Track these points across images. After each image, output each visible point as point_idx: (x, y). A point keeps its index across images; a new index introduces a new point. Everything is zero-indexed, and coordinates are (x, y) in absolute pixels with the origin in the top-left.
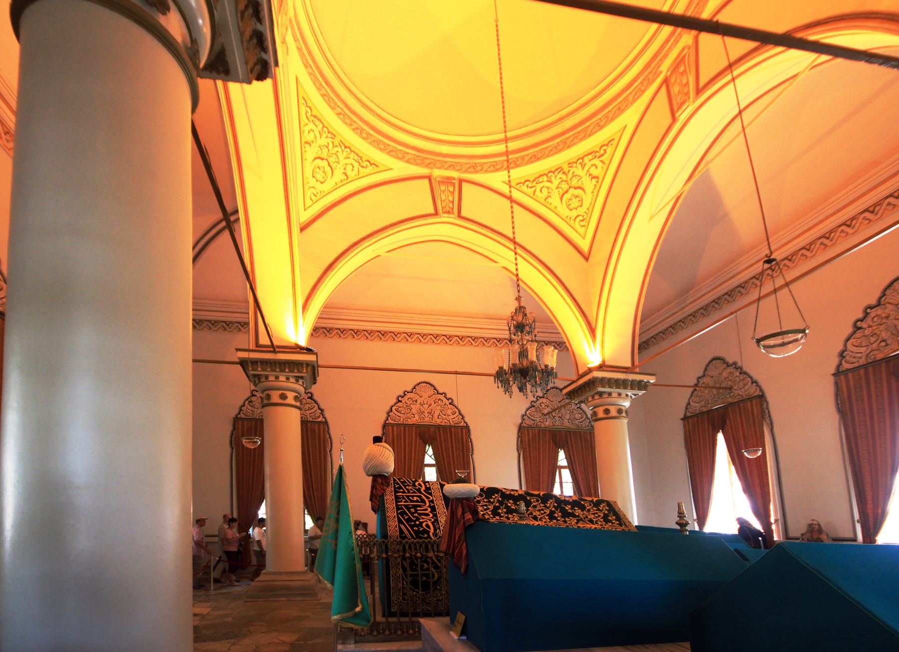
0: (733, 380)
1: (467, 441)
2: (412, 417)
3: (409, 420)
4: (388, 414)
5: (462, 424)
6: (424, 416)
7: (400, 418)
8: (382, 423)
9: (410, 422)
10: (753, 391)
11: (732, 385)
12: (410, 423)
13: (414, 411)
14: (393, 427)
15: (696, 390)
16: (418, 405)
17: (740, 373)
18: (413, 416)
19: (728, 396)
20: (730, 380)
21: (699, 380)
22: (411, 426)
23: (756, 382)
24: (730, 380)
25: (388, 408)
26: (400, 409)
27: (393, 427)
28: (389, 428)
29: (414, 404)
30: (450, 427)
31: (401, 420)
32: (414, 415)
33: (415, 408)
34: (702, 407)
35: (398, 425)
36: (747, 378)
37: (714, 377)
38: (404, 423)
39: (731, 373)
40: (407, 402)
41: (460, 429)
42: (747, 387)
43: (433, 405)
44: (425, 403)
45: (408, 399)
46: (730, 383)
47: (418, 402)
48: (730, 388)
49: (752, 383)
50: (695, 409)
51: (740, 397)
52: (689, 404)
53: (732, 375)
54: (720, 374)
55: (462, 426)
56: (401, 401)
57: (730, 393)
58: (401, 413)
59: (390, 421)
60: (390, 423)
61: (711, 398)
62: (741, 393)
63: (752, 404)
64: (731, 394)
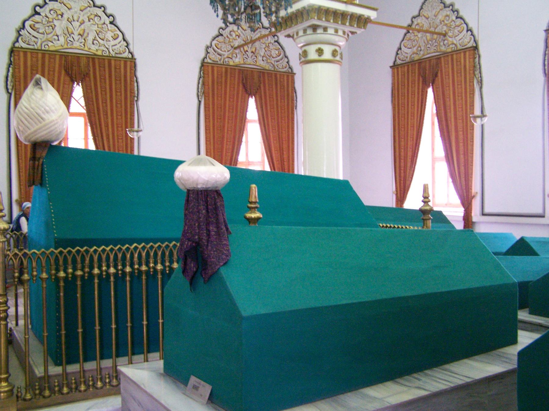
0: (449, 25)
1: (131, 81)
2: (55, 39)
3: (50, 44)
4: (18, 31)
5: (126, 55)
6: (72, 40)
7: (36, 40)
8: (9, 45)
9: (52, 47)
10: (466, 40)
11: (447, 31)
12: (51, 49)
13: (58, 31)
14: (25, 53)
15: (408, 32)
16: (65, 22)
17: (457, 18)
18: (56, 38)
19: (442, 44)
20: (446, 25)
21: (413, 20)
22: (53, 54)
23: (471, 31)
24: (446, 25)
25: (19, 24)
26: (37, 26)
27: (25, 53)
28: (19, 55)
29: (58, 20)
30: (110, 59)
31: (39, 44)
32: (58, 36)
33: (60, 26)
34: (414, 53)
35: (34, 52)
36: (462, 24)
37: (429, 19)
38: (43, 48)
39: (447, 16)
40: (48, 15)
41: (122, 63)
42: (461, 36)
43: (87, 23)
44: (76, 18)
45: (50, 10)
46: (445, 28)
47: (65, 16)
48: (445, 35)
49: (467, 31)
50: (406, 55)
51: (454, 46)
52: (400, 49)
53: (447, 18)
54: (435, 16)
55: (126, 58)
56: (39, 14)
57: (444, 41)
58: (38, 32)
59: (21, 44)
60: (22, 48)
61: (424, 44)
62: (455, 42)
63: (465, 55)
64: (446, 42)
